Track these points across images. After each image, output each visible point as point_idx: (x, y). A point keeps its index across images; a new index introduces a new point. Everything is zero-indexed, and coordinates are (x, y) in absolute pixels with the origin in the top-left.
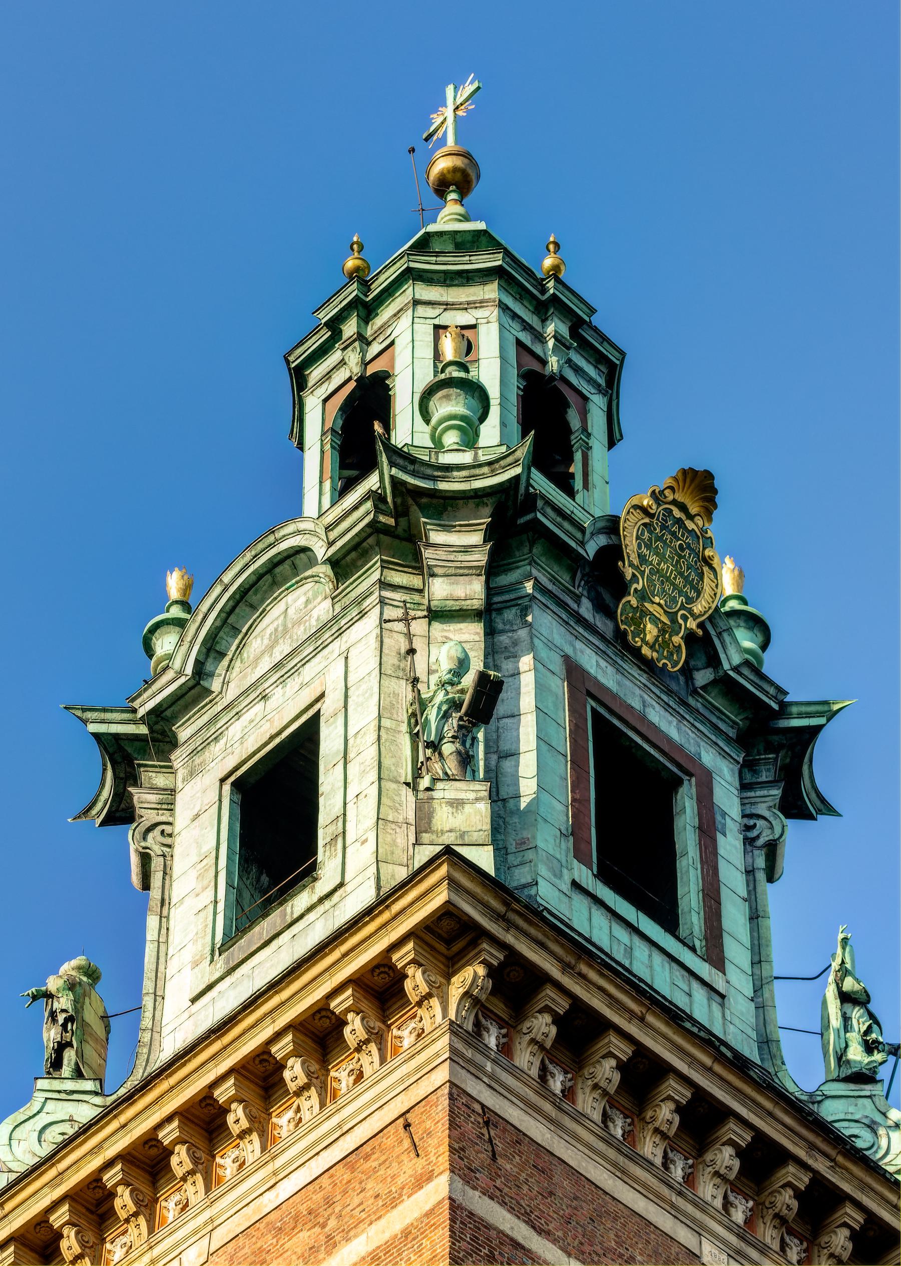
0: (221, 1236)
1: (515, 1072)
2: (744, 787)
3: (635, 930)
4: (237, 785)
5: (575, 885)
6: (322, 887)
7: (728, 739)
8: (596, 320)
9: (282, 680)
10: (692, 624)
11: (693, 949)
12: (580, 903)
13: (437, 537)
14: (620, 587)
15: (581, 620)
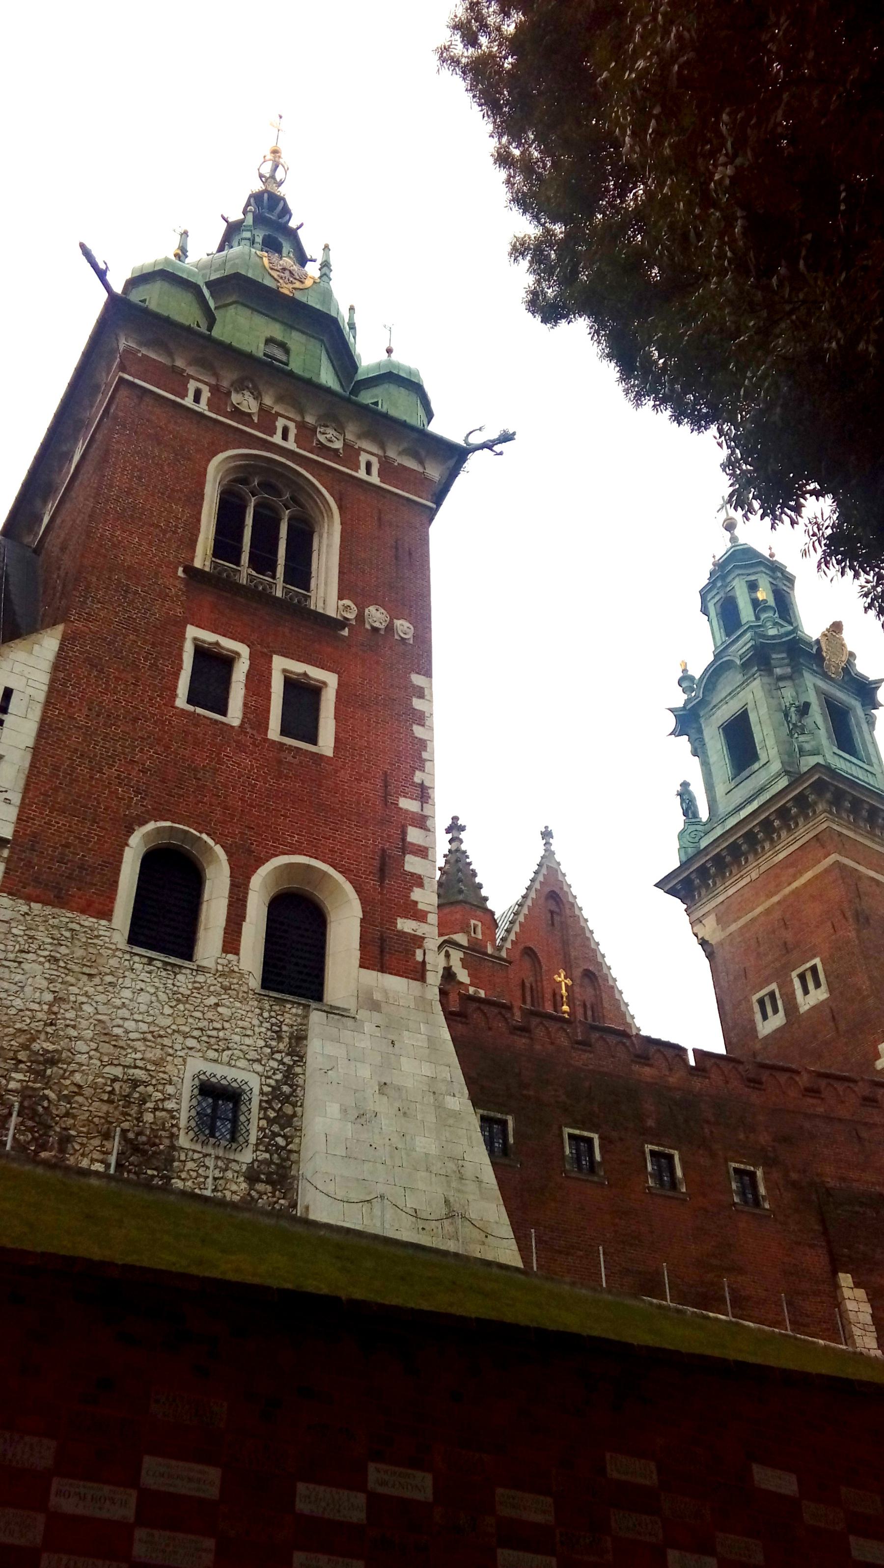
0: (763, 869)
1: (841, 818)
2: (863, 705)
3: (850, 762)
4: (723, 729)
5: (834, 753)
6: (763, 761)
7: (853, 693)
8: (787, 570)
9: (732, 698)
10: (843, 664)
11: (864, 762)
12: (836, 757)
13: (774, 656)
14: (823, 659)
15: (814, 670)
